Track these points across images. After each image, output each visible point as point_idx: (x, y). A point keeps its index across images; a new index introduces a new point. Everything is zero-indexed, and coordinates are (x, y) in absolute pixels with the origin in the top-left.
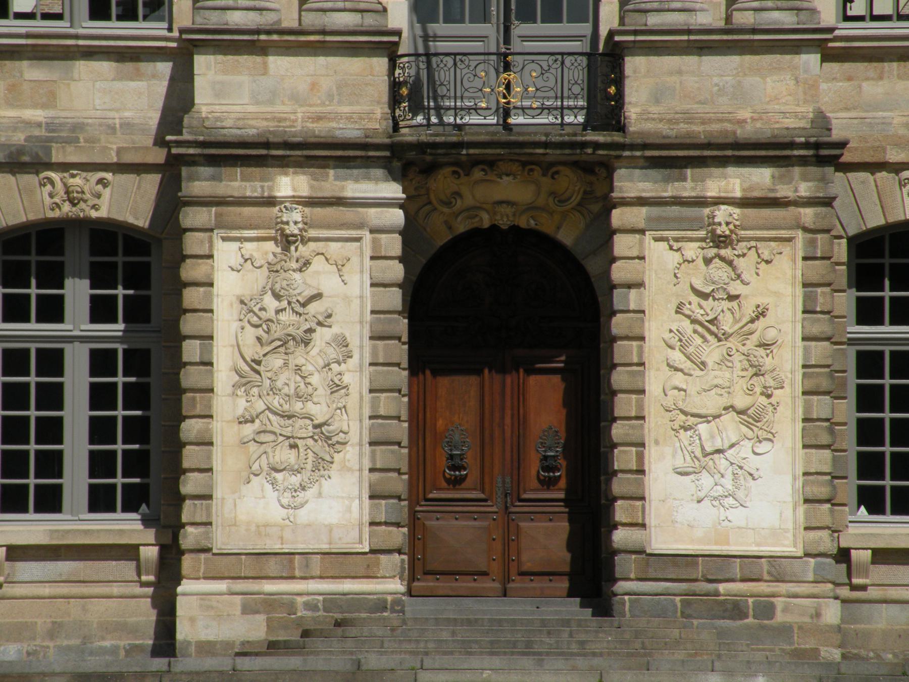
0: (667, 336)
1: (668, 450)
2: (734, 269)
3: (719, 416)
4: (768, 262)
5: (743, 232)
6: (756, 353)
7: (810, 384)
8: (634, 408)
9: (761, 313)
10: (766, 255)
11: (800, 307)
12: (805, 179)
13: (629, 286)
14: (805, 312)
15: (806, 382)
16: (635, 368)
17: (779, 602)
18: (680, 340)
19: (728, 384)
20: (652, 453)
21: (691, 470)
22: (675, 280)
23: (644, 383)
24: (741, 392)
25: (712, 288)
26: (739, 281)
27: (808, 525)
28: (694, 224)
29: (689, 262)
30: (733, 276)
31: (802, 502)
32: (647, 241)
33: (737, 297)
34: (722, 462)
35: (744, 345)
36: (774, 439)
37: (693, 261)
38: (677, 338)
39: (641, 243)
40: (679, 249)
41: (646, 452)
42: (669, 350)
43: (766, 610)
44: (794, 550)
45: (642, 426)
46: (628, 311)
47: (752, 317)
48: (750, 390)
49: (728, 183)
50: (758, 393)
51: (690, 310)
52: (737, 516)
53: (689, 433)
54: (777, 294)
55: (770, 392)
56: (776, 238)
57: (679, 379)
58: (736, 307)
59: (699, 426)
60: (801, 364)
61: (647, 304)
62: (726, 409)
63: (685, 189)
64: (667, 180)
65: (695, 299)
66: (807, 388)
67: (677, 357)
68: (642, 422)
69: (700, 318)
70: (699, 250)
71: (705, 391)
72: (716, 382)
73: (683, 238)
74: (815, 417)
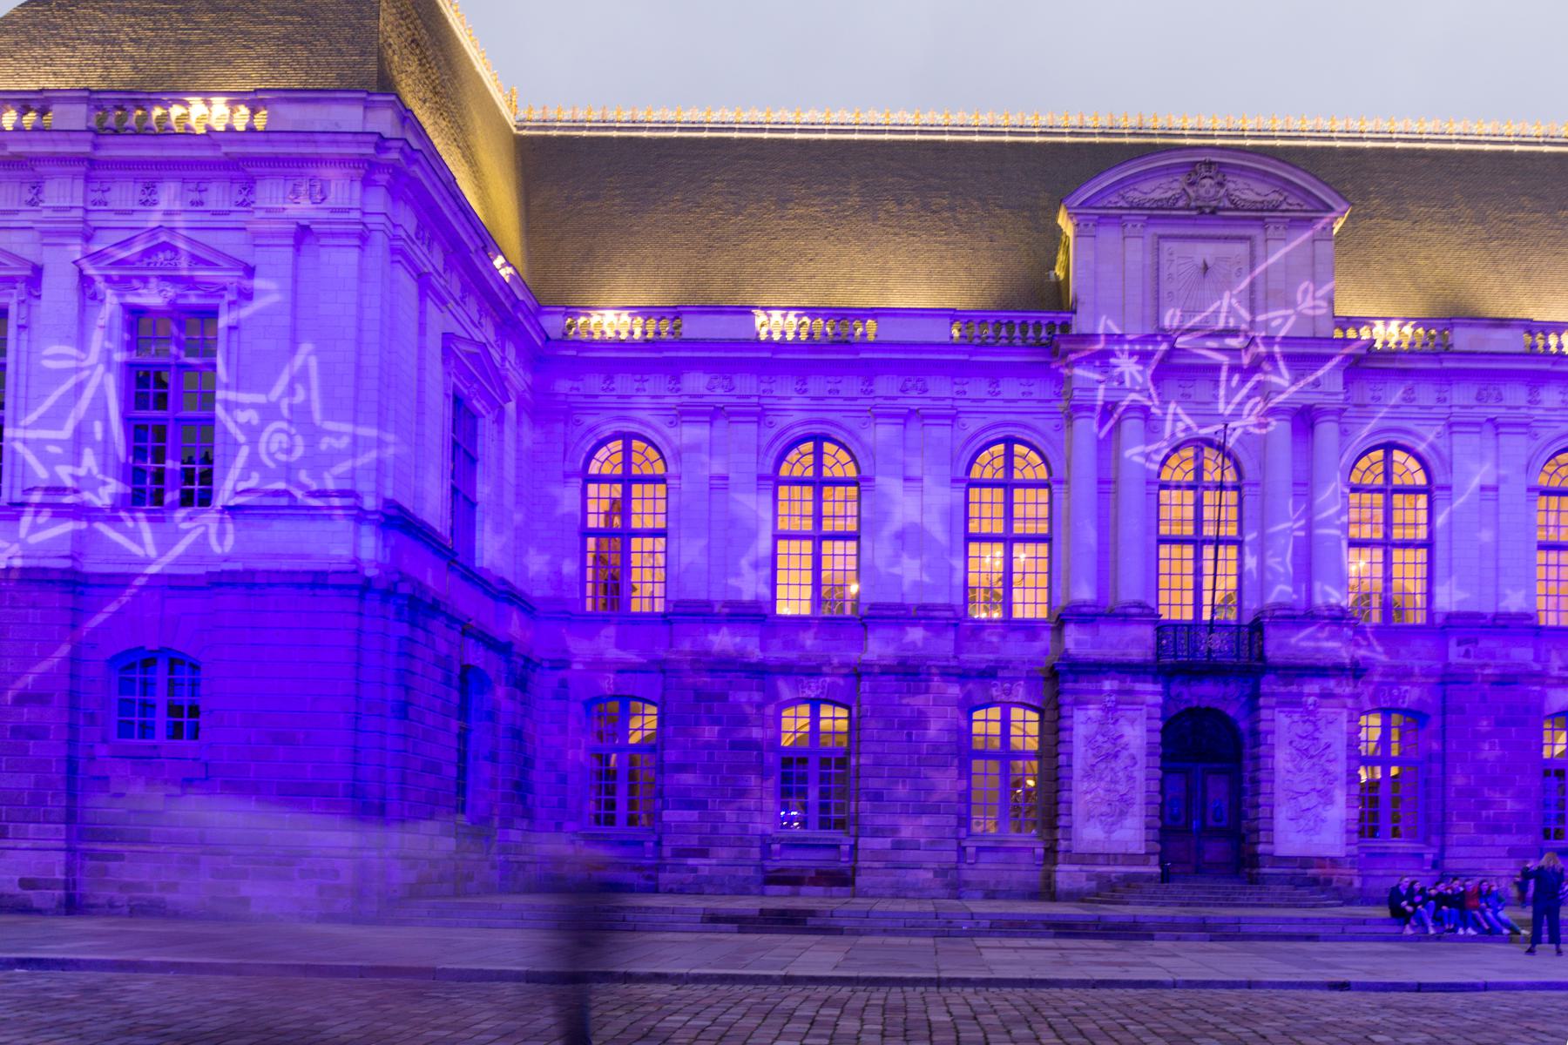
17: (1335, 878)
20: (1277, 810)
28: (1300, 704)
34: (1309, 814)
43: (1329, 882)
52: (1316, 839)
57: (1290, 776)
64: (1285, 685)
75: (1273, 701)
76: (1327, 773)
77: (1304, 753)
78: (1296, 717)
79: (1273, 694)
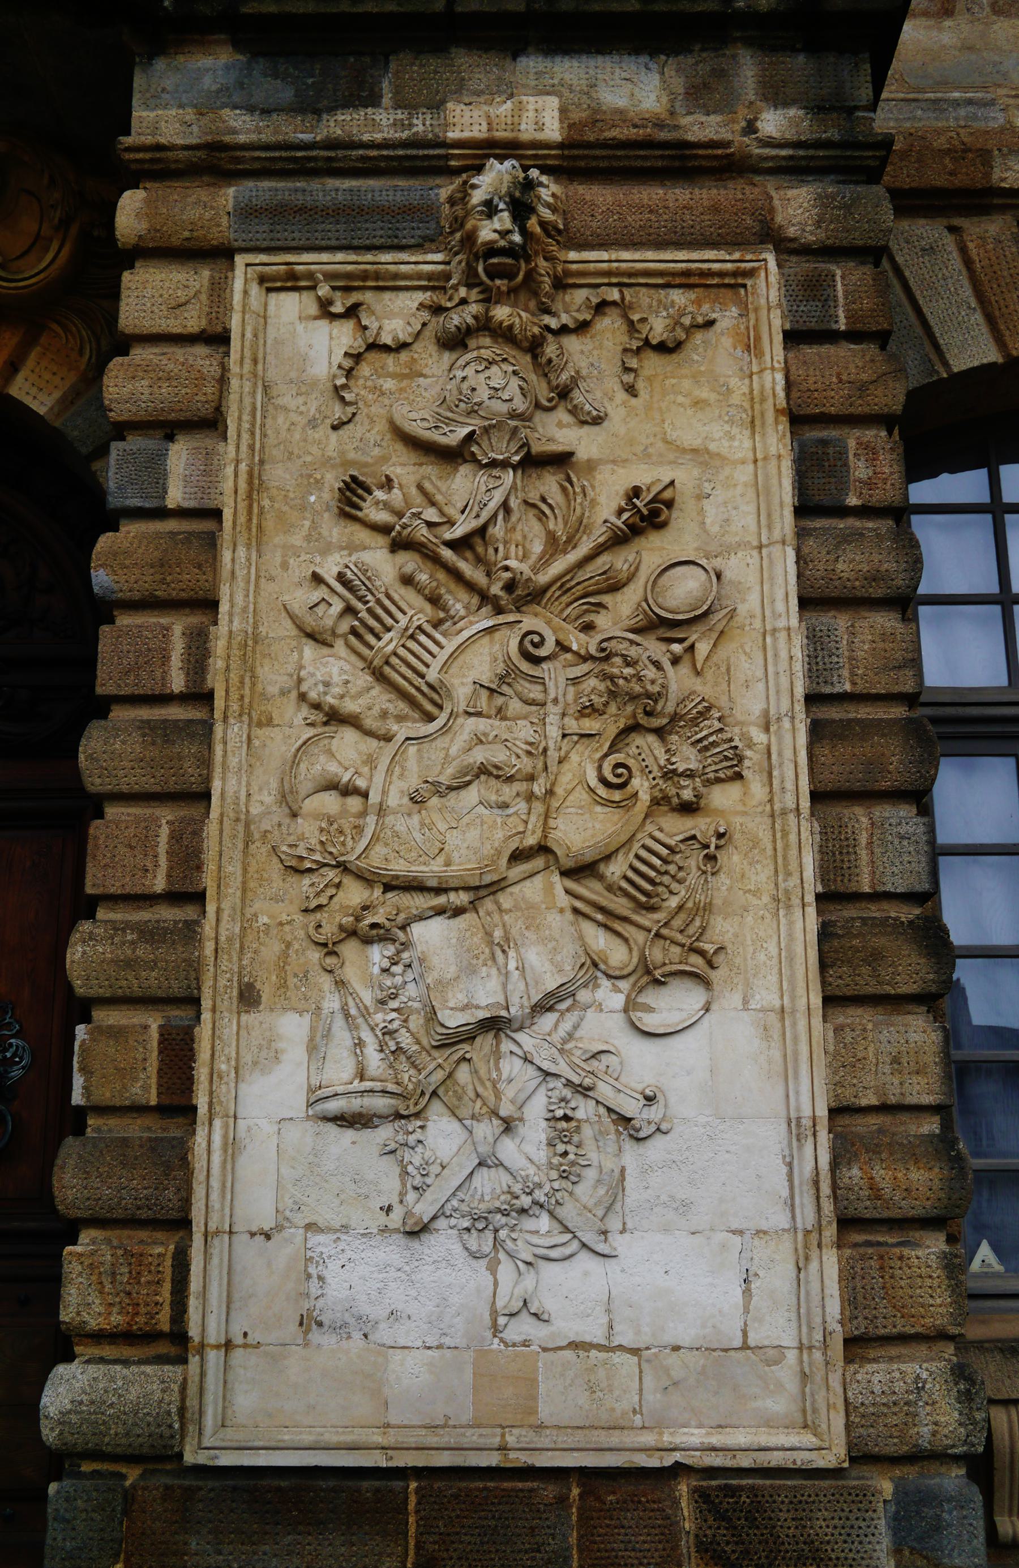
0: (302, 597)
1: (292, 1028)
2: (544, 368)
3: (497, 887)
4: (663, 348)
5: (573, 255)
6: (633, 652)
7: (844, 764)
8: (163, 861)
9: (648, 515)
10: (658, 328)
11: (785, 493)
12: (775, 95)
13: (169, 428)
14: (801, 511)
15: (824, 752)
16: (176, 712)
18: (349, 610)
19: (526, 764)
21: (381, 1104)
22: (338, 412)
23: (206, 762)
24: (581, 795)
25: (465, 431)
26: (562, 415)
27: (860, 1327)
29: (386, 348)
30: (544, 393)
31: (830, 1232)
32: (238, 285)
33: (561, 460)
35: (588, 628)
36: (714, 976)
37: (404, 346)
38: (338, 606)
39: (219, 291)
40: (352, 312)
41: (204, 1032)
42: (309, 650)
44: (808, 1439)
45: (190, 932)
46: (161, 513)
47: (613, 529)
48: (617, 783)
49: (520, 108)
50: (645, 797)
51: (387, 506)
52: (573, 1295)
53: (378, 955)
54: (702, 456)
55: (687, 795)
56: (687, 273)
58: (556, 497)
59: (417, 930)
60: (800, 691)
61: (228, 485)
62: (518, 856)
63: (375, 125)
65: (405, 469)
66: (830, 780)
67: (334, 672)
68: (189, 912)
69: (423, 533)
70: (425, 315)
71: (442, 790)
72: (479, 756)
73: (365, 276)
74: (867, 889)
75: (213, 208)
76: (647, 716)
77: (457, 562)
78: (396, 315)
79: (215, 162)
